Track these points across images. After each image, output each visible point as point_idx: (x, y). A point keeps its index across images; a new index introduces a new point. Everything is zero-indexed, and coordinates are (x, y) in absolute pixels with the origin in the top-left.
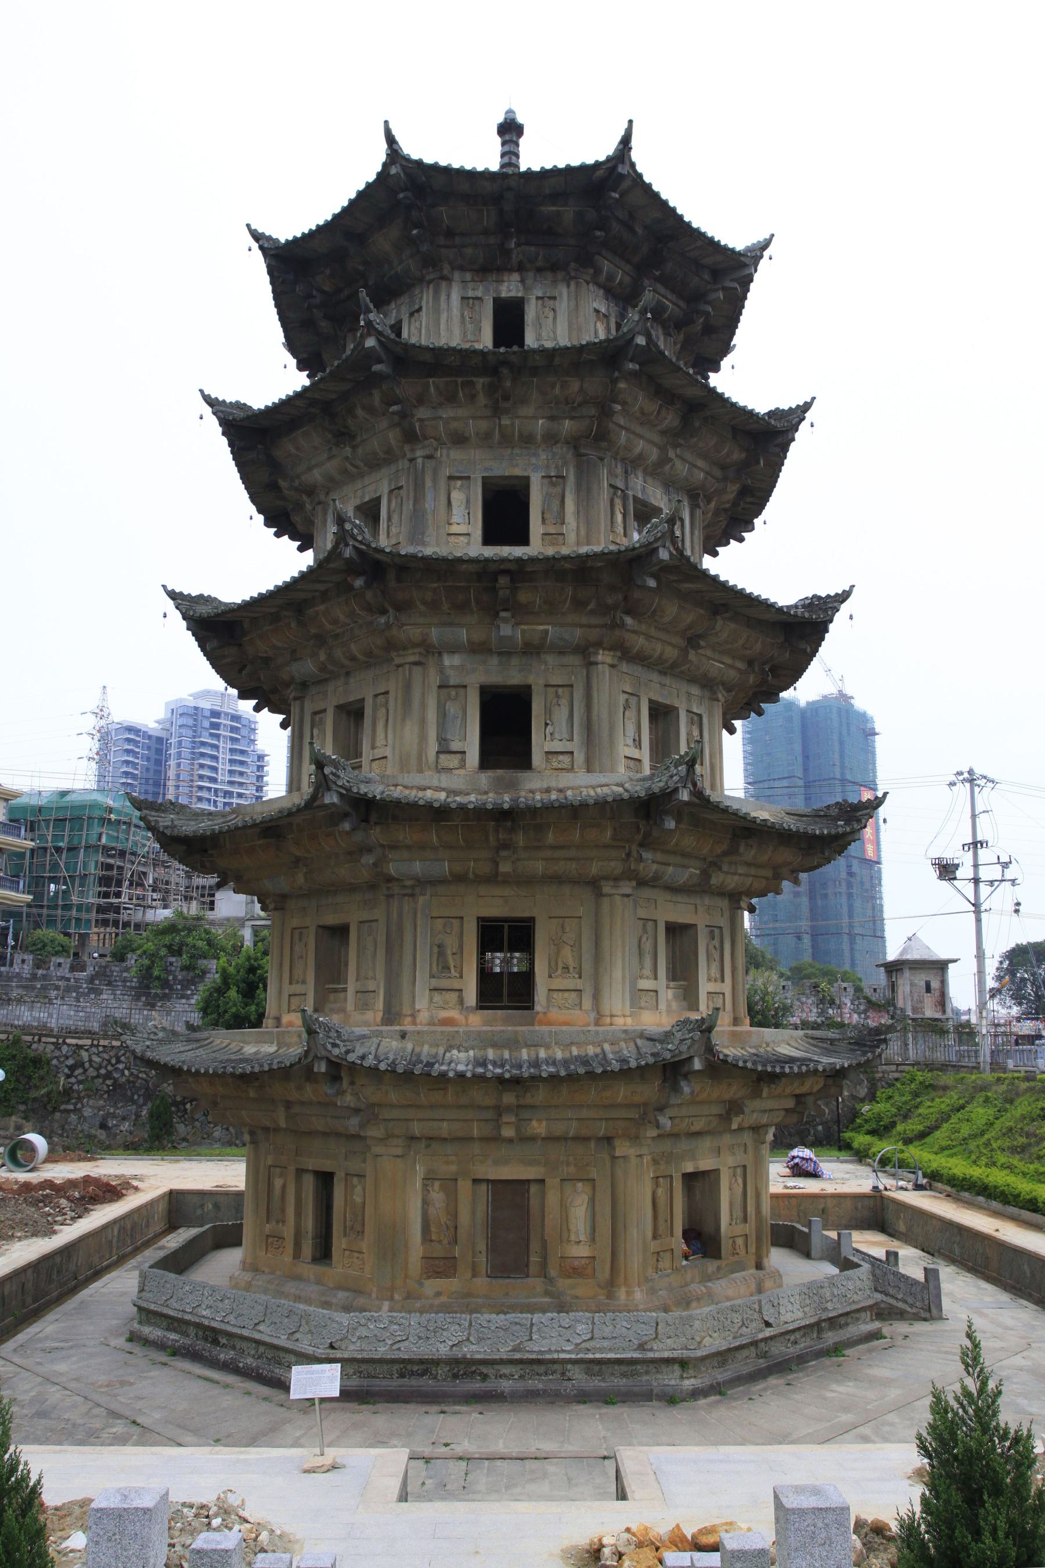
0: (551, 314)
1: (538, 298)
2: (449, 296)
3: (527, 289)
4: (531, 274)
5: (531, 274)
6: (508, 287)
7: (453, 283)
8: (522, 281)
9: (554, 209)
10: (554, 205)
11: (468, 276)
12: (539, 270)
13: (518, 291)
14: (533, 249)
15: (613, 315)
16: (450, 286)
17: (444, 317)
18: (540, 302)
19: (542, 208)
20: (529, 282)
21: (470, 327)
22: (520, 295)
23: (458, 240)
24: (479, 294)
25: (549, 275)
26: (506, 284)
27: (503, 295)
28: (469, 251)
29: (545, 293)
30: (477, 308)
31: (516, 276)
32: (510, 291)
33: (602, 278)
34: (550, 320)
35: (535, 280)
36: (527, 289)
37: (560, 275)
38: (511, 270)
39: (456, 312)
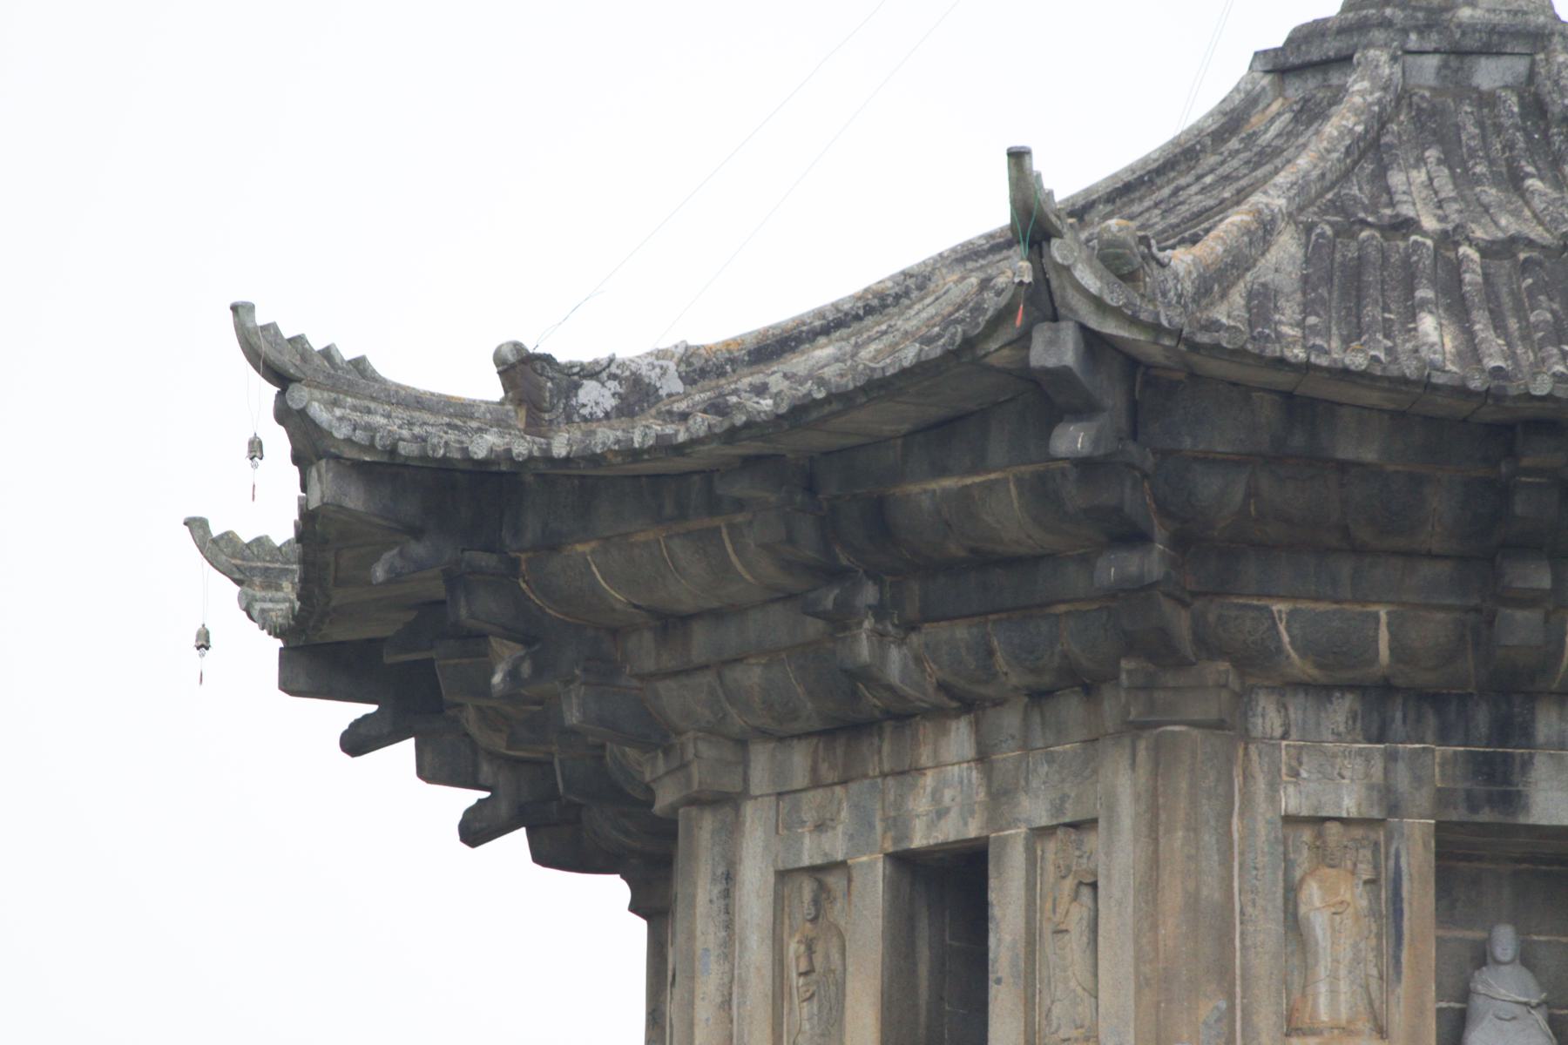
0: (1077, 916)
1: (1041, 833)
2: (729, 878)
3: (1000, 797)
4: (1010, 720)
5: (1010, 720)
6: (936, 796)
7: (749, 809)
8: (983, 757)
9: (950, 483)
10: (943, 471)
11: (799, 760)
12: (1039, 696)
13: (967, 812)
14: (962, 632)
15: (1424, 798)
16: (731, 832)
17: (708, 985)
18: (1050, 848)
19: (914, 489)
20: (1007, 756)
21: (803, 1015)
22: (973, 831)
23: (701, 642)
24: (835, 845)
25: (1071, 708)
26: (929, 780)
27: (919, 840)
28: (751, 676)
29: (1058, 809)
30: (837, 912)
31: (959, 739)
32: (941, 813)
33: (1299, 665)
34: (1076, 940)
35: (1026, 747)
36: (1000, 797)
37: (1111, 706)
38: (939, 715)
39: (756, 950)
